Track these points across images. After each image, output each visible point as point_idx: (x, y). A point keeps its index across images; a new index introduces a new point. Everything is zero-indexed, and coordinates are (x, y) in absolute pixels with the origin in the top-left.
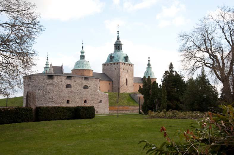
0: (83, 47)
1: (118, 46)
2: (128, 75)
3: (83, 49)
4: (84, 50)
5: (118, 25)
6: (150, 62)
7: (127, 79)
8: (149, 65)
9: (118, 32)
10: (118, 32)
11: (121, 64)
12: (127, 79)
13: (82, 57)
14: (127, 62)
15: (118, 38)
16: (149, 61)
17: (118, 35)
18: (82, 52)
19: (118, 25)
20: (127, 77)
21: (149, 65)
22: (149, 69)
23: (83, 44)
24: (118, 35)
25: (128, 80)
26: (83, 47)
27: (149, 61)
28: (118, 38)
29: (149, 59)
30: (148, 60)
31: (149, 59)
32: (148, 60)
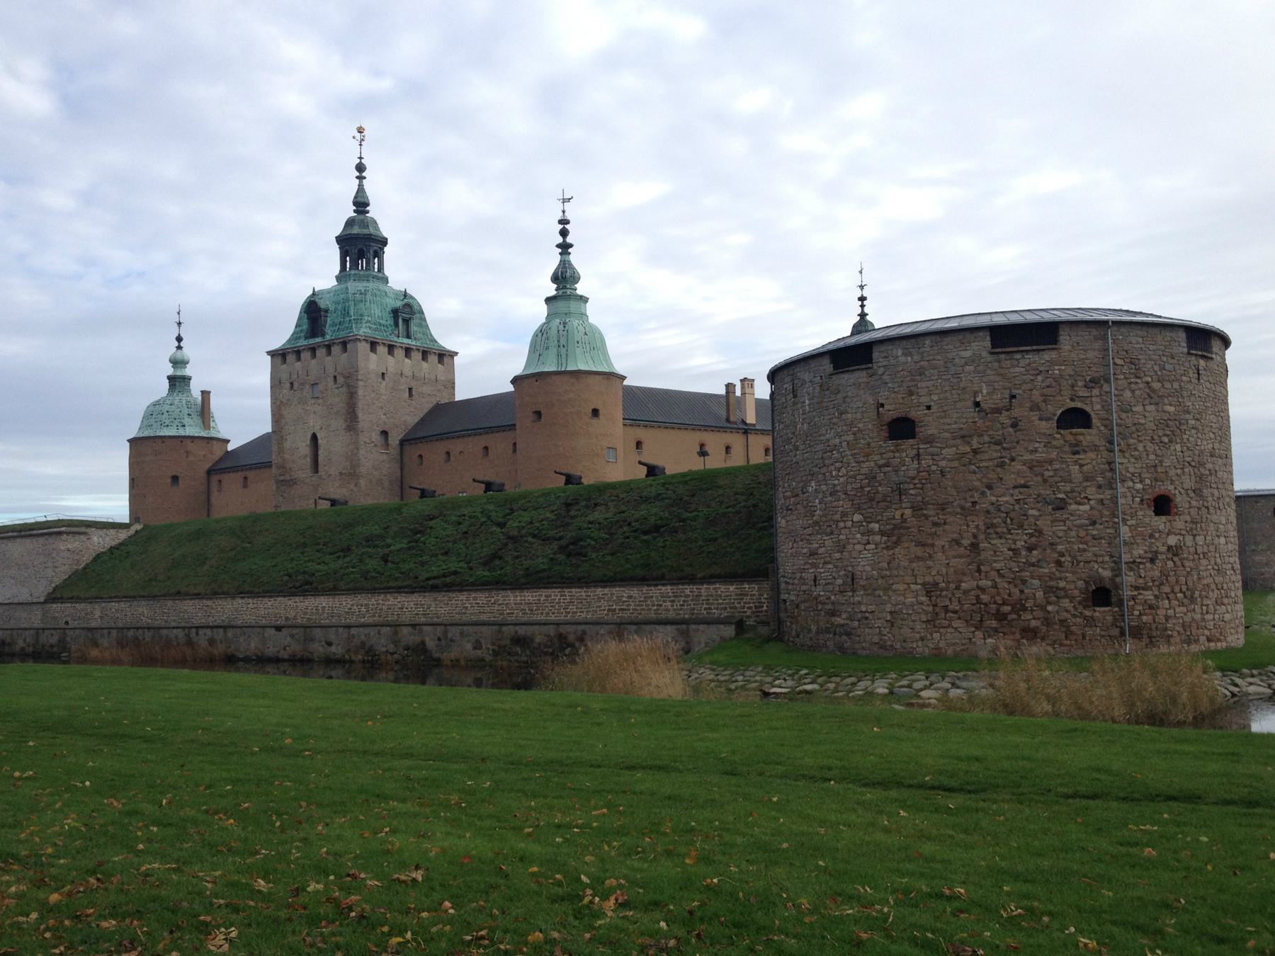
0: (179, 339)
1: (360, 245)
2: (319, 408)
3: (179, 348)
4: (188, 351)
5: (360, 130)
6: (575, 257)
7: (314, 438)
8: (564, 277)
9: (360, 168)
10: (360, 168)
11: (364, 347)
12: (314, 438)
13: (178, 382)
14: (312, 341)
15: (361, 204)
16: (565, 248)
17: (361, 189)
18: (177, 363)
19: (360, 130)
20: (314, 424)
21: (564, 277)
22: (573, 305)
23: (179, 324)
24: (361, 189)
25: (320, 441)
26: (179, 339)
27: (565, 248)
28: (361, 204)
29: (564, 233)
30: (560, 240)
31: (564, 233)
32: (560, 240)
